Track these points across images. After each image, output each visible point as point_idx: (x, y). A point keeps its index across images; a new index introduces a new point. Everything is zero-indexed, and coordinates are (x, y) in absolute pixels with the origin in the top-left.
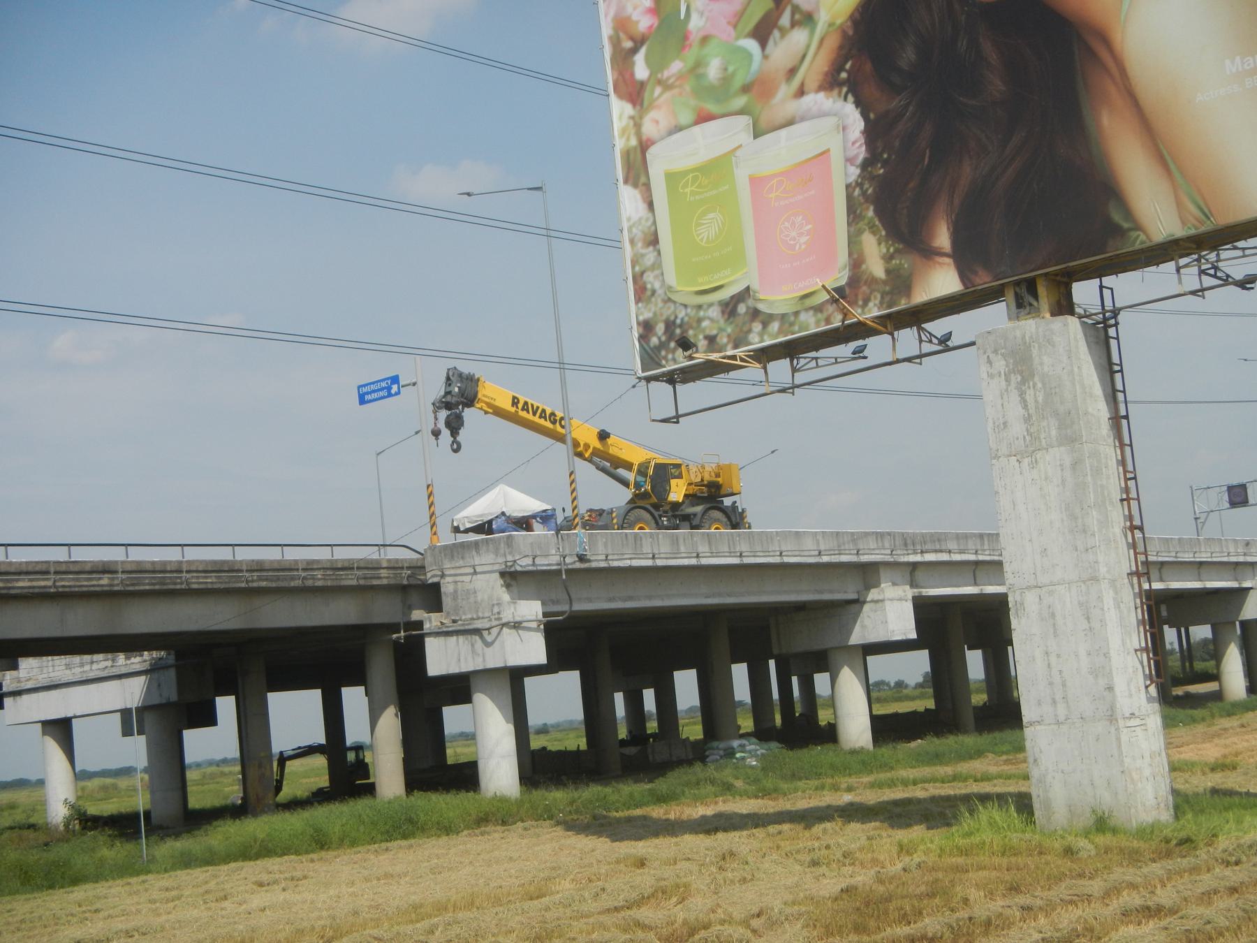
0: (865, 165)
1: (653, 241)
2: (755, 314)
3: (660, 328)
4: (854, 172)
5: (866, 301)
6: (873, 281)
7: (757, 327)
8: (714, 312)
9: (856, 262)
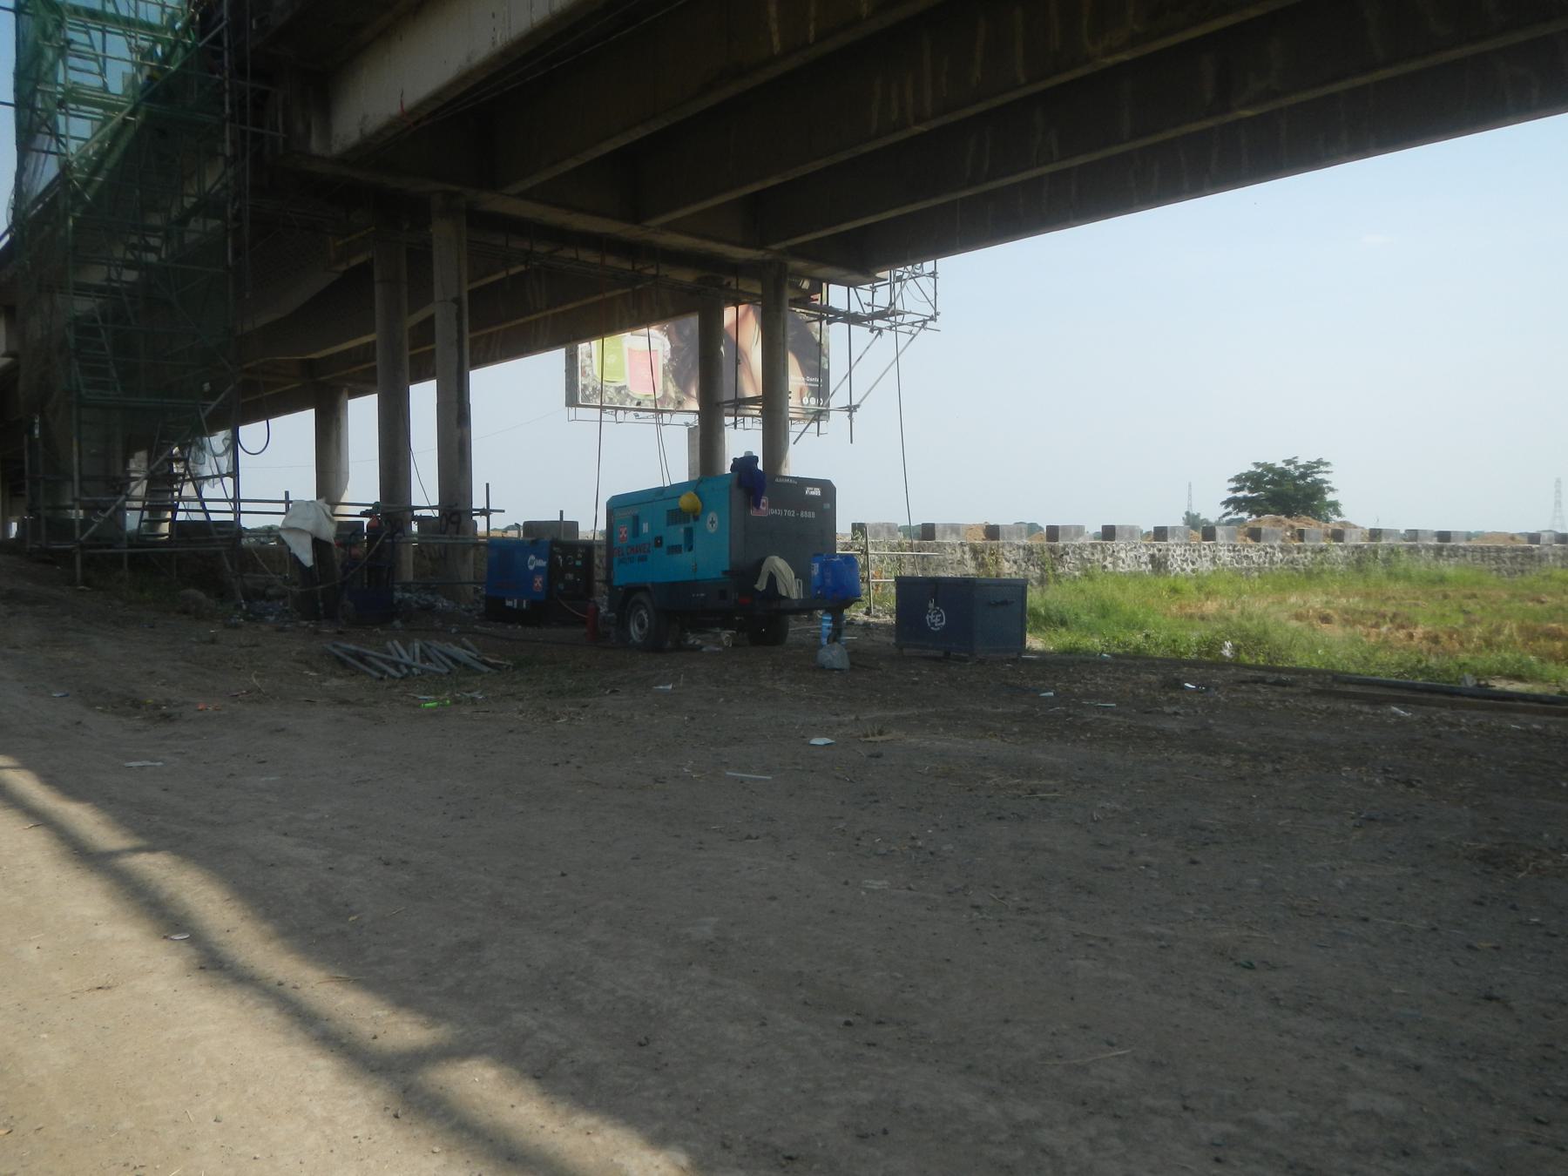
0: (670, 360)
1: (590, 356)
2: (628, 395)
3: (590, 389)
4: (666, 361)
5: (668, 405)
6: (671, 398)
7: (629, 400)
8: (612, 390)
9: (665, 391)
